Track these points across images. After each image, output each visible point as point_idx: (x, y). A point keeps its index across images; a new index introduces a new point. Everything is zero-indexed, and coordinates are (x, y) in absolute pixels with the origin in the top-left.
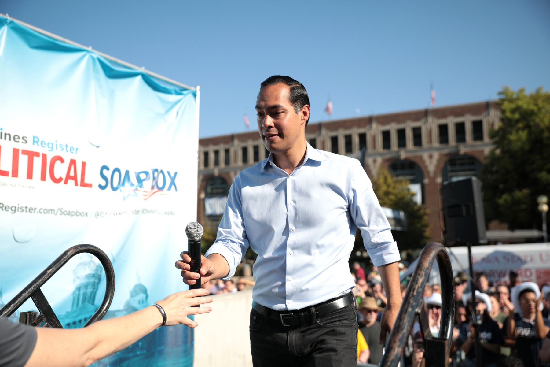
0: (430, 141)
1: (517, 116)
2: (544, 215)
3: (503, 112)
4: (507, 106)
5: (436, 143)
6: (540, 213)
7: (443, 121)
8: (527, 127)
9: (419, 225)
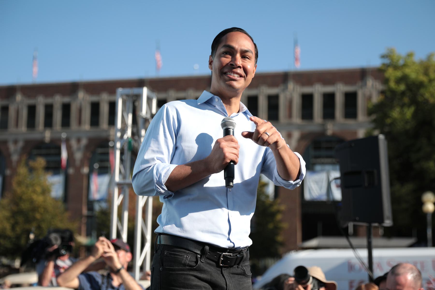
0: (290, 116)
1: (402, 87)
2: (429, 219)
3: (386, 81)
4: (391, 73)
5: (297, 120)
6: (424, 215)
7: (307, 90)
8: (414, 102)
9: (271, 226)
